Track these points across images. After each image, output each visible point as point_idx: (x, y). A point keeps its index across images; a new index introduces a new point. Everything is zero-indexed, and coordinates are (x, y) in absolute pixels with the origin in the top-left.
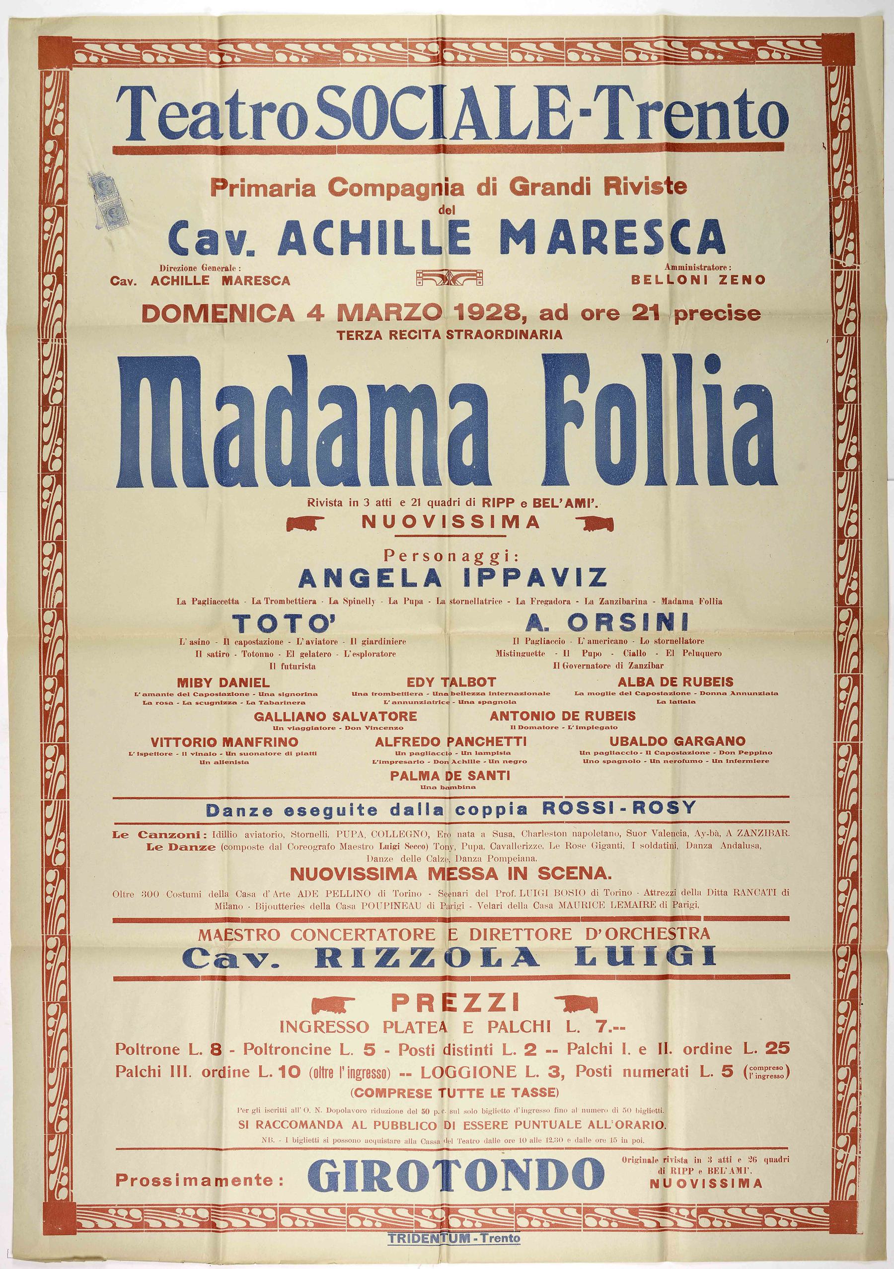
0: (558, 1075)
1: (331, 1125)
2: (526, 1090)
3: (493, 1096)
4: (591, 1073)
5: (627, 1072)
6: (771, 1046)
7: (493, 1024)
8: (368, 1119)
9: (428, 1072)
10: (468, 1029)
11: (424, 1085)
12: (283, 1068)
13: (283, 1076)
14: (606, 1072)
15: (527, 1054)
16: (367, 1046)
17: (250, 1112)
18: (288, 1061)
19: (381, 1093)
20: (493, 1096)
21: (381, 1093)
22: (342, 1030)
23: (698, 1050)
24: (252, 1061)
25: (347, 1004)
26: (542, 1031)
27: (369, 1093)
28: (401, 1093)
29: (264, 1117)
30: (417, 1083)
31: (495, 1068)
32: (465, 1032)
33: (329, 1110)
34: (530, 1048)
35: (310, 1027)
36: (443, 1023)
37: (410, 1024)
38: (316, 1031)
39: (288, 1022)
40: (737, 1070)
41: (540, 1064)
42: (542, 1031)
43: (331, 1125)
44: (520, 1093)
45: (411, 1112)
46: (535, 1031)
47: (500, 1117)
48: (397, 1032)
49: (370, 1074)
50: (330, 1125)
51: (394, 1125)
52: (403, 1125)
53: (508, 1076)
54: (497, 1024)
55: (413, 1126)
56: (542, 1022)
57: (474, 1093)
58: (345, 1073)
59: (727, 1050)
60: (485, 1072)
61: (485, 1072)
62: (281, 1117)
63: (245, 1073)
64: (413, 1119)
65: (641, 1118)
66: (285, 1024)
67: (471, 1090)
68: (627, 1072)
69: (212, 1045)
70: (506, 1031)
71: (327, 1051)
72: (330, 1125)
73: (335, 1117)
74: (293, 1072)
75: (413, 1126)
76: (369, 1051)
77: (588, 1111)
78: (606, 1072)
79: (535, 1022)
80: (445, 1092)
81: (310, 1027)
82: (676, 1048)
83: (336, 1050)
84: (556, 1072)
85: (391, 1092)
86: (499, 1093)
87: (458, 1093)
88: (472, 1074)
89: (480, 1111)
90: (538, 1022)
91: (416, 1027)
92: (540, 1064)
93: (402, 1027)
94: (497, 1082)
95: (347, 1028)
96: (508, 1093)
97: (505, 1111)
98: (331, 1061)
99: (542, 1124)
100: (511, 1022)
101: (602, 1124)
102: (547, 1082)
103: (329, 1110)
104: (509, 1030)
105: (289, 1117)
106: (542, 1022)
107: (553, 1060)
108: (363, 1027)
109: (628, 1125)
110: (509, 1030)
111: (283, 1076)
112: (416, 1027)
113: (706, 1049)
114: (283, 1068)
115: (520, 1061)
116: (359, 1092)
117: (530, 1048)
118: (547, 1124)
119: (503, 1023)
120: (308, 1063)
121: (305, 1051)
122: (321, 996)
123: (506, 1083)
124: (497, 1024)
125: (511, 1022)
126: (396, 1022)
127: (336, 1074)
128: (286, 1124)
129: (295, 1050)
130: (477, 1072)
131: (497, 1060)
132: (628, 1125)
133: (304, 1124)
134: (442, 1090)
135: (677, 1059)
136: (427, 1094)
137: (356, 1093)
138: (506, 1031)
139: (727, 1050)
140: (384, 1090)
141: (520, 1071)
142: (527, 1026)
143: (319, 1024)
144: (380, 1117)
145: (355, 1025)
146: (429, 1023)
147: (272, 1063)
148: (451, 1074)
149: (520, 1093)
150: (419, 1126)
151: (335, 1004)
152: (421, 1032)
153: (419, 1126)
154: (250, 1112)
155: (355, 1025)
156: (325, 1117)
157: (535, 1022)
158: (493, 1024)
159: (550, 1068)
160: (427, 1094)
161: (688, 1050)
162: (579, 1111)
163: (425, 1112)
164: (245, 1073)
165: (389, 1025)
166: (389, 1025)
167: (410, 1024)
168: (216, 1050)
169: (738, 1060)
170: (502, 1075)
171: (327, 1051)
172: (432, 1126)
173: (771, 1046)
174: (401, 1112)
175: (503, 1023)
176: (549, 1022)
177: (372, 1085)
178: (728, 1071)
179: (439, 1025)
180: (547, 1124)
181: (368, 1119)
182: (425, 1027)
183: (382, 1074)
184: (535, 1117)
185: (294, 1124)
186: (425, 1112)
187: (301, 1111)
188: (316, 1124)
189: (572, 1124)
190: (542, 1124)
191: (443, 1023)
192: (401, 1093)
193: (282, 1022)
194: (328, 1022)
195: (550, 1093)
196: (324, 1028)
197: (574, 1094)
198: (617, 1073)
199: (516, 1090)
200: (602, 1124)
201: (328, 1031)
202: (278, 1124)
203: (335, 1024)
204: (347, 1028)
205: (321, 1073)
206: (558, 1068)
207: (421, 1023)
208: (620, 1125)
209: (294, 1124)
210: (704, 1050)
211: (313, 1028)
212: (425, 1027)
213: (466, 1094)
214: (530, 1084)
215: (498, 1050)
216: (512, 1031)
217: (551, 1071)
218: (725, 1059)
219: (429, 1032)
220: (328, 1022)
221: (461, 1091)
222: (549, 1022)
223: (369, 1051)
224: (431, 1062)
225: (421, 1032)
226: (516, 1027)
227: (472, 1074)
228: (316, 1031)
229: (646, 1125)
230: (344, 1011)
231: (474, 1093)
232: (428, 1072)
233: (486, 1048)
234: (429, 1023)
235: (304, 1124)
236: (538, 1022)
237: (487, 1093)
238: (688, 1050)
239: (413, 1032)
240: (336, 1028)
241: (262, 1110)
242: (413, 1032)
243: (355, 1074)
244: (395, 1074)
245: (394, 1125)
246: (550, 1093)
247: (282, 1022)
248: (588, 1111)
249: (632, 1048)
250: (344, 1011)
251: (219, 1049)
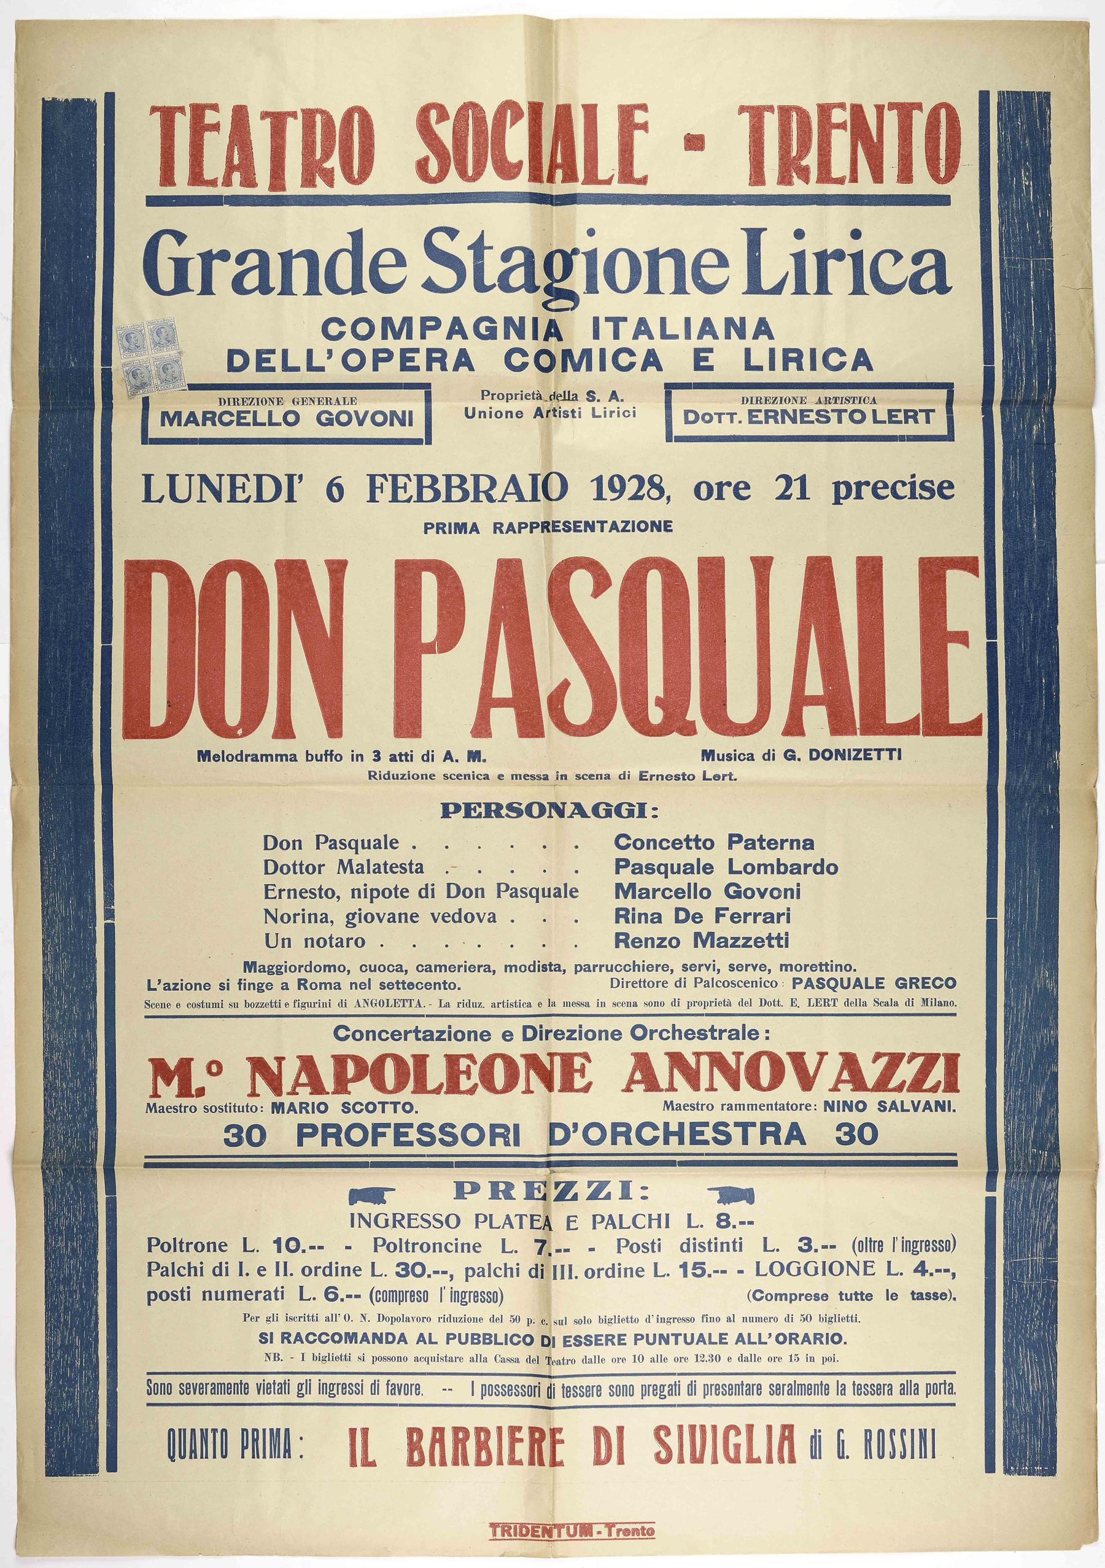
7: (599, 1219)
10: (572, 1225)
22: (427, 1225)
25: (387, 1195)
26: (659, 1226)
32: (568, 1228)
35: (387, 1220)
37: (508, 1217)
38: (394, 1226)
39: (360, 1215)
42: (659, 1226)
46: (650, 1227)
48: (491, 1227)
54: (603, 1218)
56: (659, 1215)
66: (356, 1217)
70: (615, 1227)
79: (650, 1215)
81: (387, 1220)
90: (655, 1216)
91: (516, 1222)
95: (433, 1222)
100: (621, 1216)
106: (659, 1215)
108: (453, 1221)
112: (516, 1222)
119: (610, 1216)
122: (359, 1187)
124: (603, 1218)
125: (621, 1216)
126: (491, 1215)
129: (437, 1246)
138: (615, 1227)
142: (641, 1222)
143: (399, 1217)
145: (443, 1219)
146: (532, 1216)
151: (375, 1195)
152: (521, 1227)
155: (443, 1219)
157: (650, 1215)
166: (481, 1218)
167: (508, 1217)
175: (610, 1216)
176: (667, 1215)
179: (542, 1220)
193: (352, 1215)
194: (409, 1215)
196: (405, 1222)
201: (409, 1226)
203: (419, 1218)
204: (433, 1222)
207: (521, 1216)
211: (391, 1222)
212: (526, 1221)
216: (621, 1227)
219: (532, 1227)
220: (409, 1215)
222: (667, 1215)
225: (521, 1227)
226: (628, 1221)
228: (394, 1226)
230: (384, 1202)
234: (532, 1216)
236: (655, 1216)
239: (512, 1227)
240: (420, 1222)
242: (512, 1227)
247: (352, 1215)
250: (384, 1202)
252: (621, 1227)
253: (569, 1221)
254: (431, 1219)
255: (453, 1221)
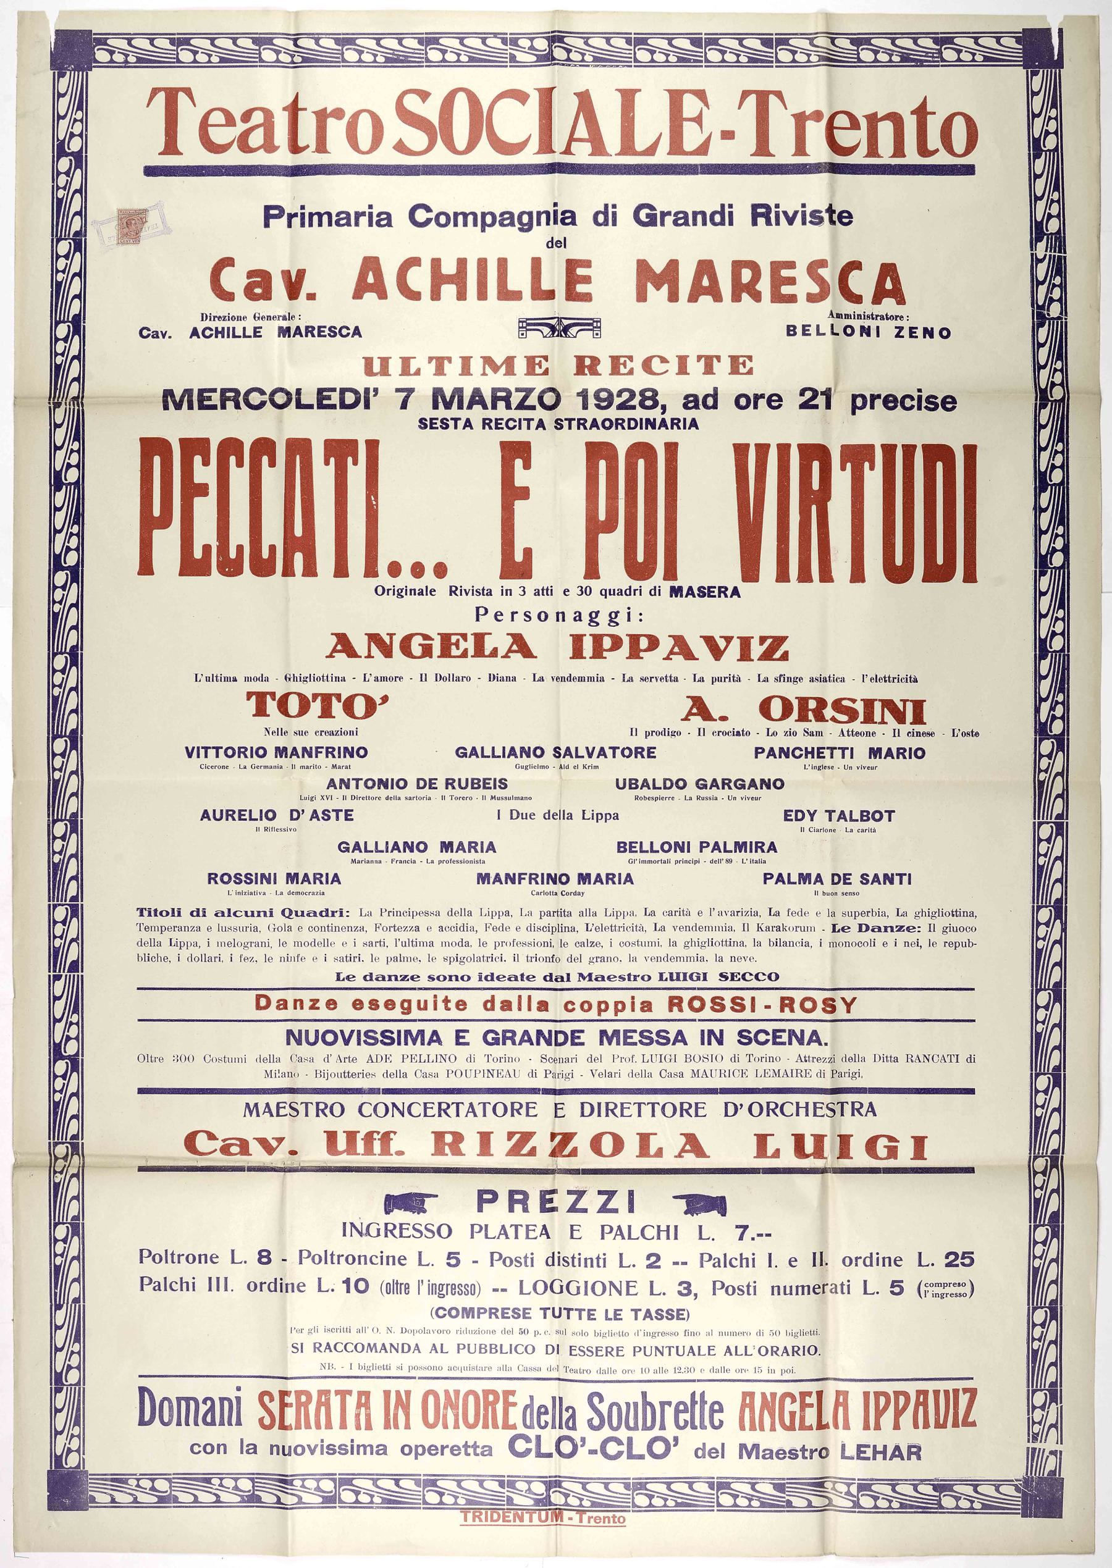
0: (690, 1292)
1: (406, 1348)
2: (648, 1311)
3: (607, 1319)
4: (730, 1290)
5: (776, 1290)
6: (952, 1257)
7: (607, 1229)
8: (450, 1344)
9: (528, 1288)
10: (576, 1234)
11: (521, 1302)
12: (347, 1282)
13: (348, 1291)
14: (749, 1290)
15: (649, 1266)
16: (450, 1255)
17: (305, 1331)
18: (354, 1272)
19: (468, 1312)
20: (607, 1319)
21: (468, 1312)
22: (418, 1234)
23: (860, 1262)
24: (307, 1273)
27: (454, 1313)
28: (493, 1312)
29: (324, 1338)
30: (513, 1300)
31: (611, 1283)
33: (403, 1331)
34: (653, 1259)
36: (544, 1227)
40: (910, 1288)
41: (667, 1278)
43: (406, 1348)
44: (641, 1315)
45: (505, 1332)
47: (614, 1342)
49: (454, 1289)
50: (405, 1349)
51: (482, 1349)
52: (494, 1349)
53: (628, 1294)
55: (506, 1349)
57: (585, 1314)
58: (424, 1288)
59: (897, 1262)
60: (599, 1288)
61: (599, 1288)
62: (344, 1338)
63: (300, 1288)
64: (506, 1341)
65: (790, 1342)
66: (348, 1226)
67: (580, 1311)
68: (776, 1290)
69: (260, 1252)
71: (401, 1261)
72: (405, 1349)
73: (411, 1340)
74: (359, 1286)
75: (506, 1349)
76: (453, 1262)
77: (727, 1334)
78: (749, 1290)
80: (549, 1312)
82: (834, 1258)
83: (412, 1260)
84: (686, 1288)
85: (481, 1311)
86: (615, 1314)
87: (564, 1313)
88: (582, 1290)
89: (592, 1334)
90: (664, 1228)
91: (511, 1232)
92: (667, 1278)
93: (494, 1231)
94: (612, 1301)
96: (628, 1315)
97: (622, 1334)
98: (408, 1274)
99: (666, 1351)
101: (741, 1351)
102: (674, 1302)
103: (403, 1331)
104: (626, 1235)
105: (354, 1338)
107: (684, 1274)
108: (444, 1231)
109: (774, 1351)
110: (626, 1235)
111: (348, 1291)
112: (511, 1232)
113: (871, 1260)
114: (347, 1282)
115: (641, 1275)
116: (441, 1313)
117: (653, 1259)
118: (673, 1351)
119: (619, 1228)
120: (378, 1275)
121: (374, 1260)
122: (396, 1192)
123: (625, 1303)
127: (413, 1288)
128: (350, 1347)
130: (590, 1288)
131: (612, 1273)
132: (774, 1351)
133: (372, 1347)
134: (545, 1310)
135: (837, 1273)
136: (525, 1314)
137: (438, 1313)
139: (897, 1262)
140: (472, 1309)
141: (643, 1288)
142: (650, 1232)
143: (390, 1227)
144: (465, 1339)
147: (334, 1274)
148: (557, 1288)
149: (641, 1315)
150: (514, 1349)
151: (412, 1202)
153: (514, 1349)
154: (305, 1331)
155: (435, 1229)
156: (397, 1339)
158: (607, 1229)
159: (680, 1284)
160: (525, 1314)
161: (847, 1261)
162: (716, 1333)
163: (523, 1332)
164: (300, 1288)
165: (477, 1228)
166: (477, 1228)
168: (264, 1257)
169: (909, 1274)
170: (620, 1293)
171: (401, 1261)
172: (530, 1349)
173: (952, 1257)
174: (494, 1332)
175: (619, 1228)
177: (454, 1301)
178: (897, 1287)
179: (539, 1229)
180: (673, 1351)
181: (450, 1344)
182: (522, 1231)
183: (471, 1290)
184: (660, 1342)
185: (359, 1348)
186: (523, 1332)
187: (369, 1331)
188: (388, 1347)
189: (704, 1350)
190: (666, 1351)
191: (544, 1227)
192: (493, 1312)
195: (678, 1315)
196: (397, 1232)
197: (711, 1314)
198: (764, 1289)
199: (636, 1311)
200: (741, 1351)
202: (340, 1347)
205: (396, 1288)
206: (689, 1284)
207: (516, 1226)
208: (763, 1351)
209: (359, 1348)
210: (868, 1262)
211: (382, 1232)
212: (522, 1231)
213: (574, 1315)
214: (654, 1303)
215: (613, 1261)
216: (630, 1238)
217: (681, 1288)
218: (894, 1273)
219: (527, 1237)
221: (569, 1310)
223: (453, 1262)
224: (529, 1275)
226: (636, 1233)
227: (582, 1290)
229: (795, 1351)
230: (425, 1211)
231: (585, 1314)
232: (528, 1288)
233: (598, 1258)
235: (372, 1347)
236: (664, 1228)
237: (599, 1315)
238: (847, 1261)
240: (411, 1232)
241: (321, 1329)
243: (437, 1290)
244: (486, 1290)
245: (482, 1349)
246: (678, 1315)
248: (727, 1334)
249: (781, 1260)
250: (425, 1211)
251: (268, 1257)
252: (630, 1238)
253: (572, 1230)
254: (422, 1229)
255: (444, 1231)
